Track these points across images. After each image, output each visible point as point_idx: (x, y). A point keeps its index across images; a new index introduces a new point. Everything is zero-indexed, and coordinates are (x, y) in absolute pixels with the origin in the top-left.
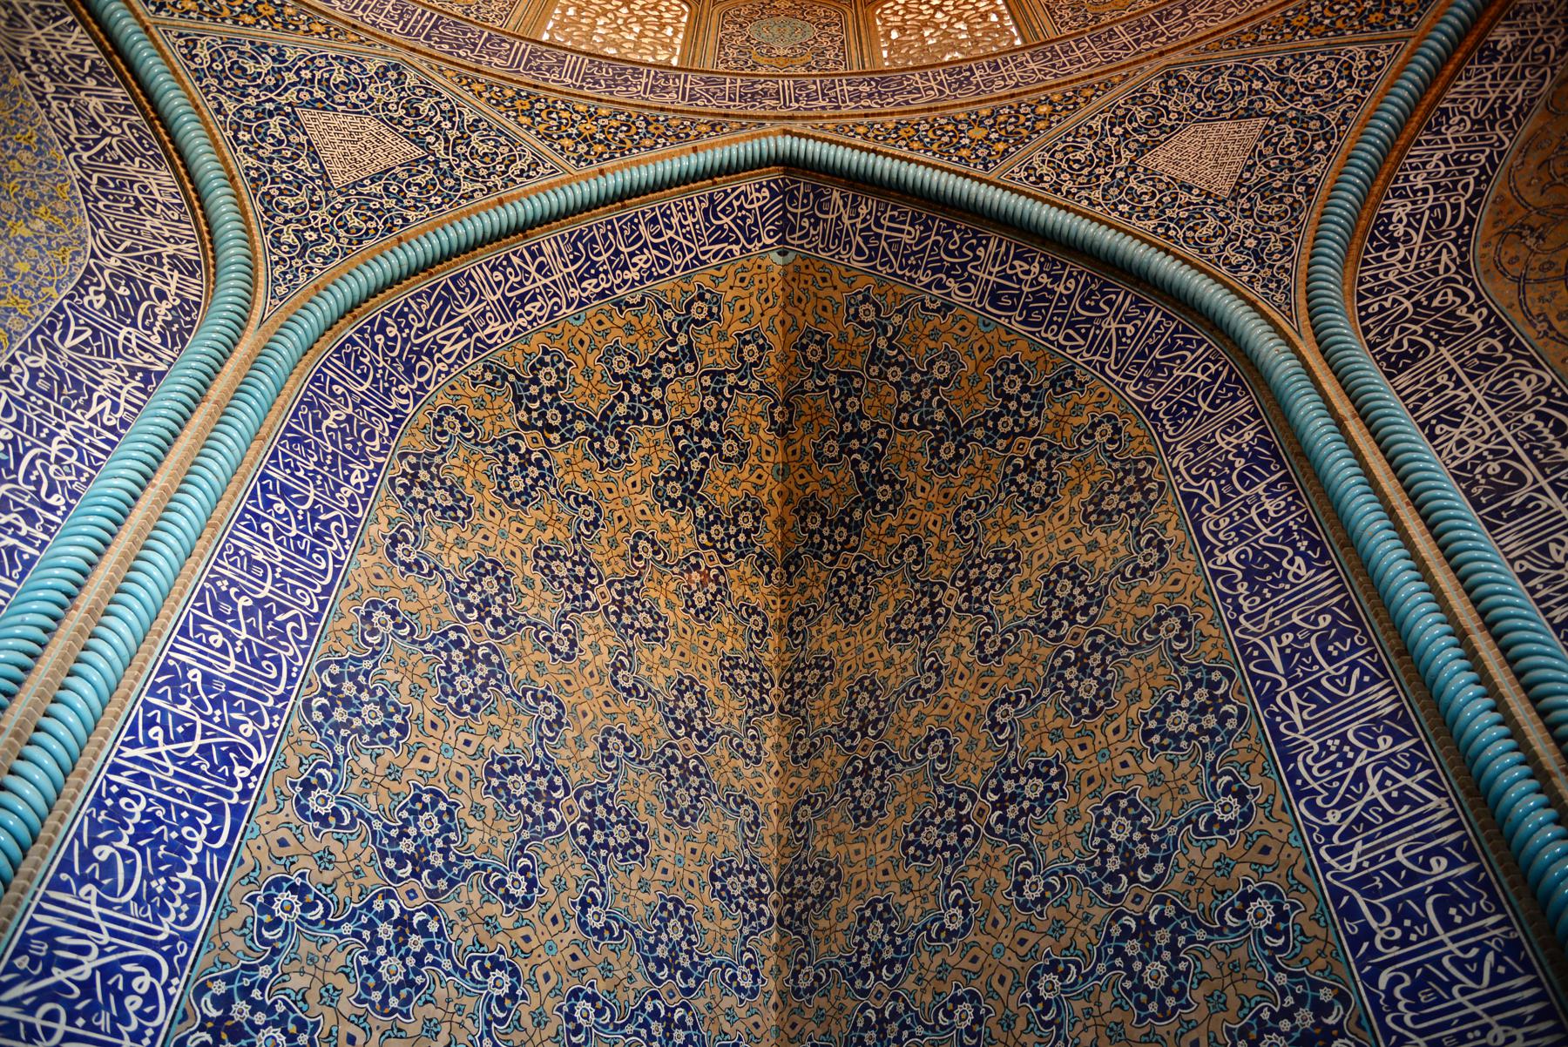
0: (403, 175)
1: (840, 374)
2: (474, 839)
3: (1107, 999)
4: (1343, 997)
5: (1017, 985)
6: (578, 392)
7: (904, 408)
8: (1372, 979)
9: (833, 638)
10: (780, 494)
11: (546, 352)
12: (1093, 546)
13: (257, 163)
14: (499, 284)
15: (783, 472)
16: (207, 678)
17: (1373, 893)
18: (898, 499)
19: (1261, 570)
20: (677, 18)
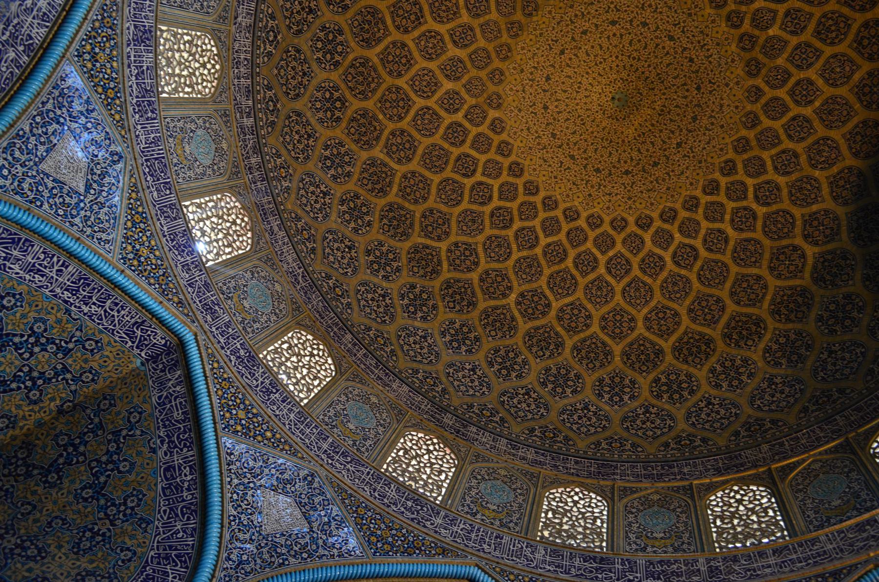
1: (101, 422)
6: (11, 317)
10: (29, 429)
11: (20, 294)
13: (28, 131)
14: (38, 258)
15: (40, 424)
18: (53, 485)
20: (239, 248)
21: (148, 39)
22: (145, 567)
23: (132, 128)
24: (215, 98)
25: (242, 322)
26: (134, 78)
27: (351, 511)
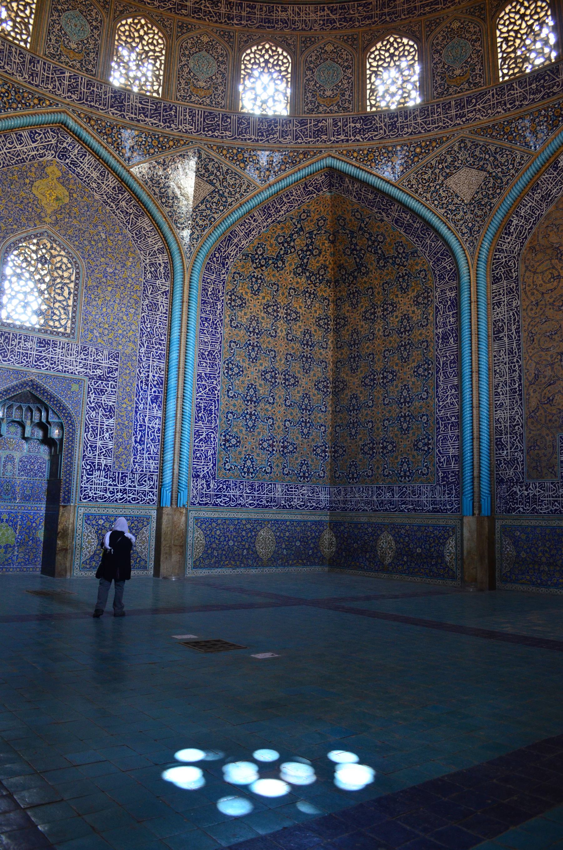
0: (210, 199)
2: (261, 392)
3: (396, 428)
4: (432, 438)
5: (380, 422)
7: (369, 246)
8: (437, 436)
9: (348, 311)
12: (413, 312)
16: (205, 374)
17: (442, 421)
18: (367, 273)
19: (445, 337)
21: (120, 96)
22: (434, 273)
23: (180, 134)
24: (167, 37)
25: (339, 106)
26: (147, 119)
27: (502, 137)
